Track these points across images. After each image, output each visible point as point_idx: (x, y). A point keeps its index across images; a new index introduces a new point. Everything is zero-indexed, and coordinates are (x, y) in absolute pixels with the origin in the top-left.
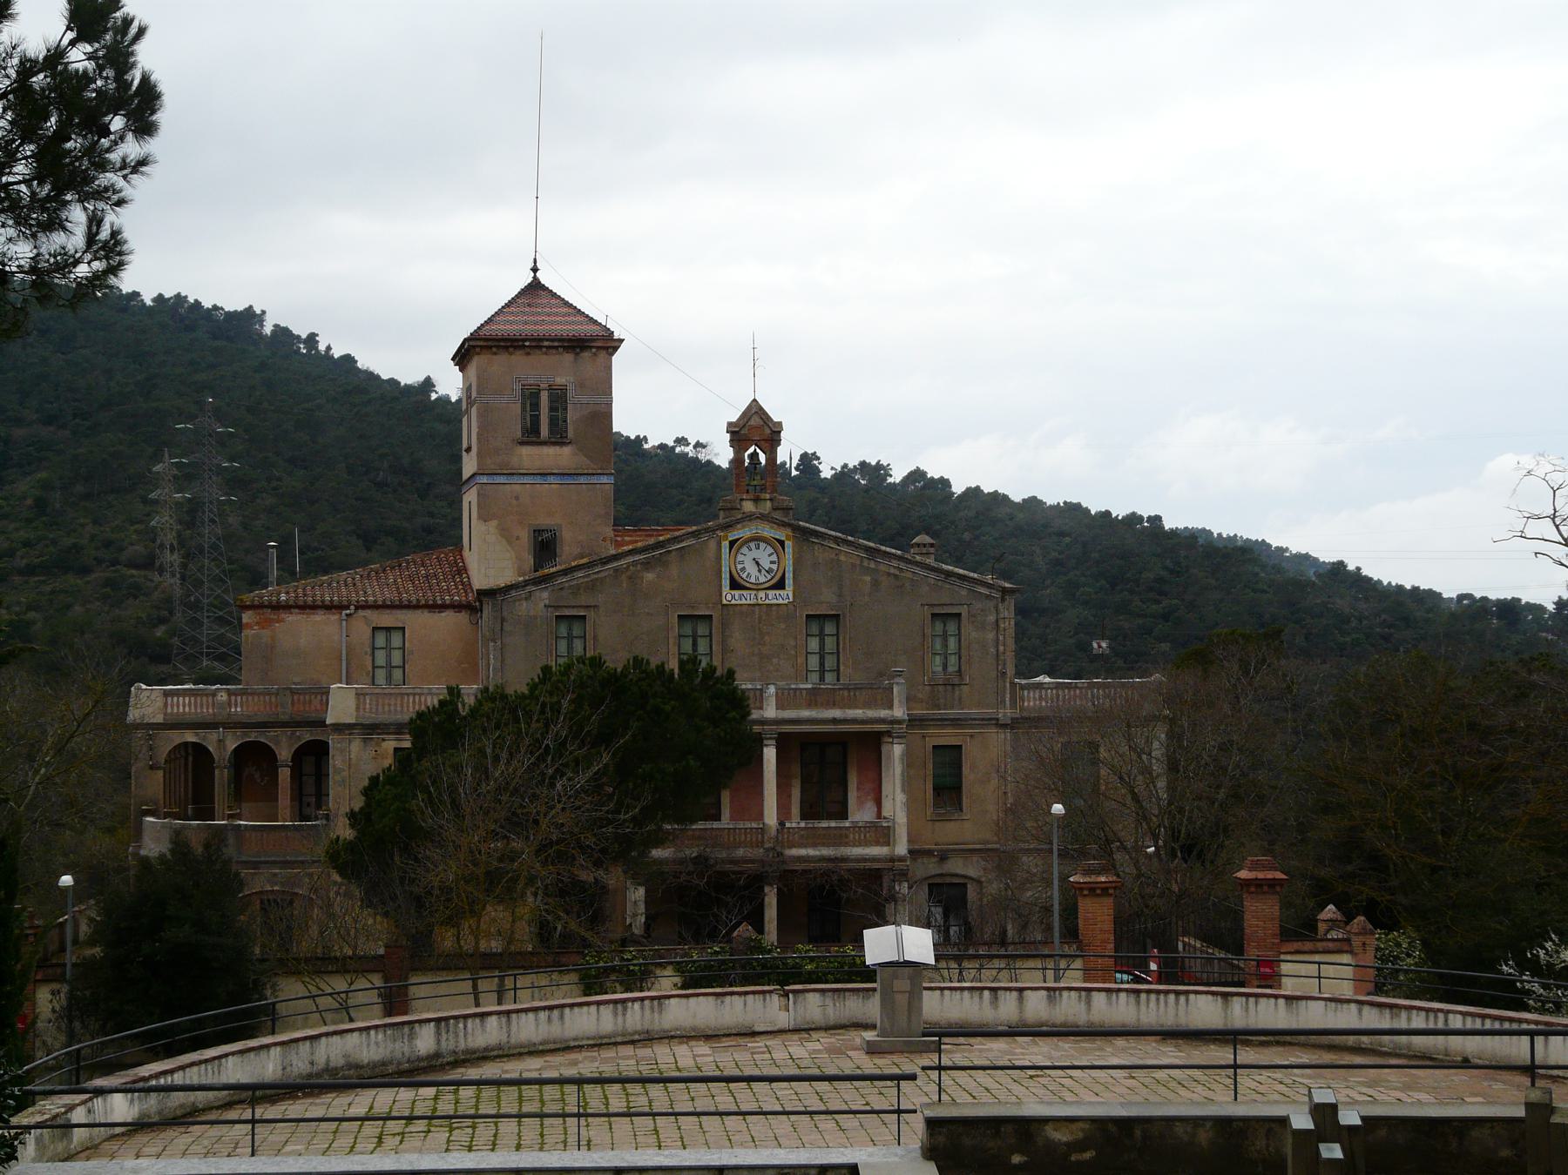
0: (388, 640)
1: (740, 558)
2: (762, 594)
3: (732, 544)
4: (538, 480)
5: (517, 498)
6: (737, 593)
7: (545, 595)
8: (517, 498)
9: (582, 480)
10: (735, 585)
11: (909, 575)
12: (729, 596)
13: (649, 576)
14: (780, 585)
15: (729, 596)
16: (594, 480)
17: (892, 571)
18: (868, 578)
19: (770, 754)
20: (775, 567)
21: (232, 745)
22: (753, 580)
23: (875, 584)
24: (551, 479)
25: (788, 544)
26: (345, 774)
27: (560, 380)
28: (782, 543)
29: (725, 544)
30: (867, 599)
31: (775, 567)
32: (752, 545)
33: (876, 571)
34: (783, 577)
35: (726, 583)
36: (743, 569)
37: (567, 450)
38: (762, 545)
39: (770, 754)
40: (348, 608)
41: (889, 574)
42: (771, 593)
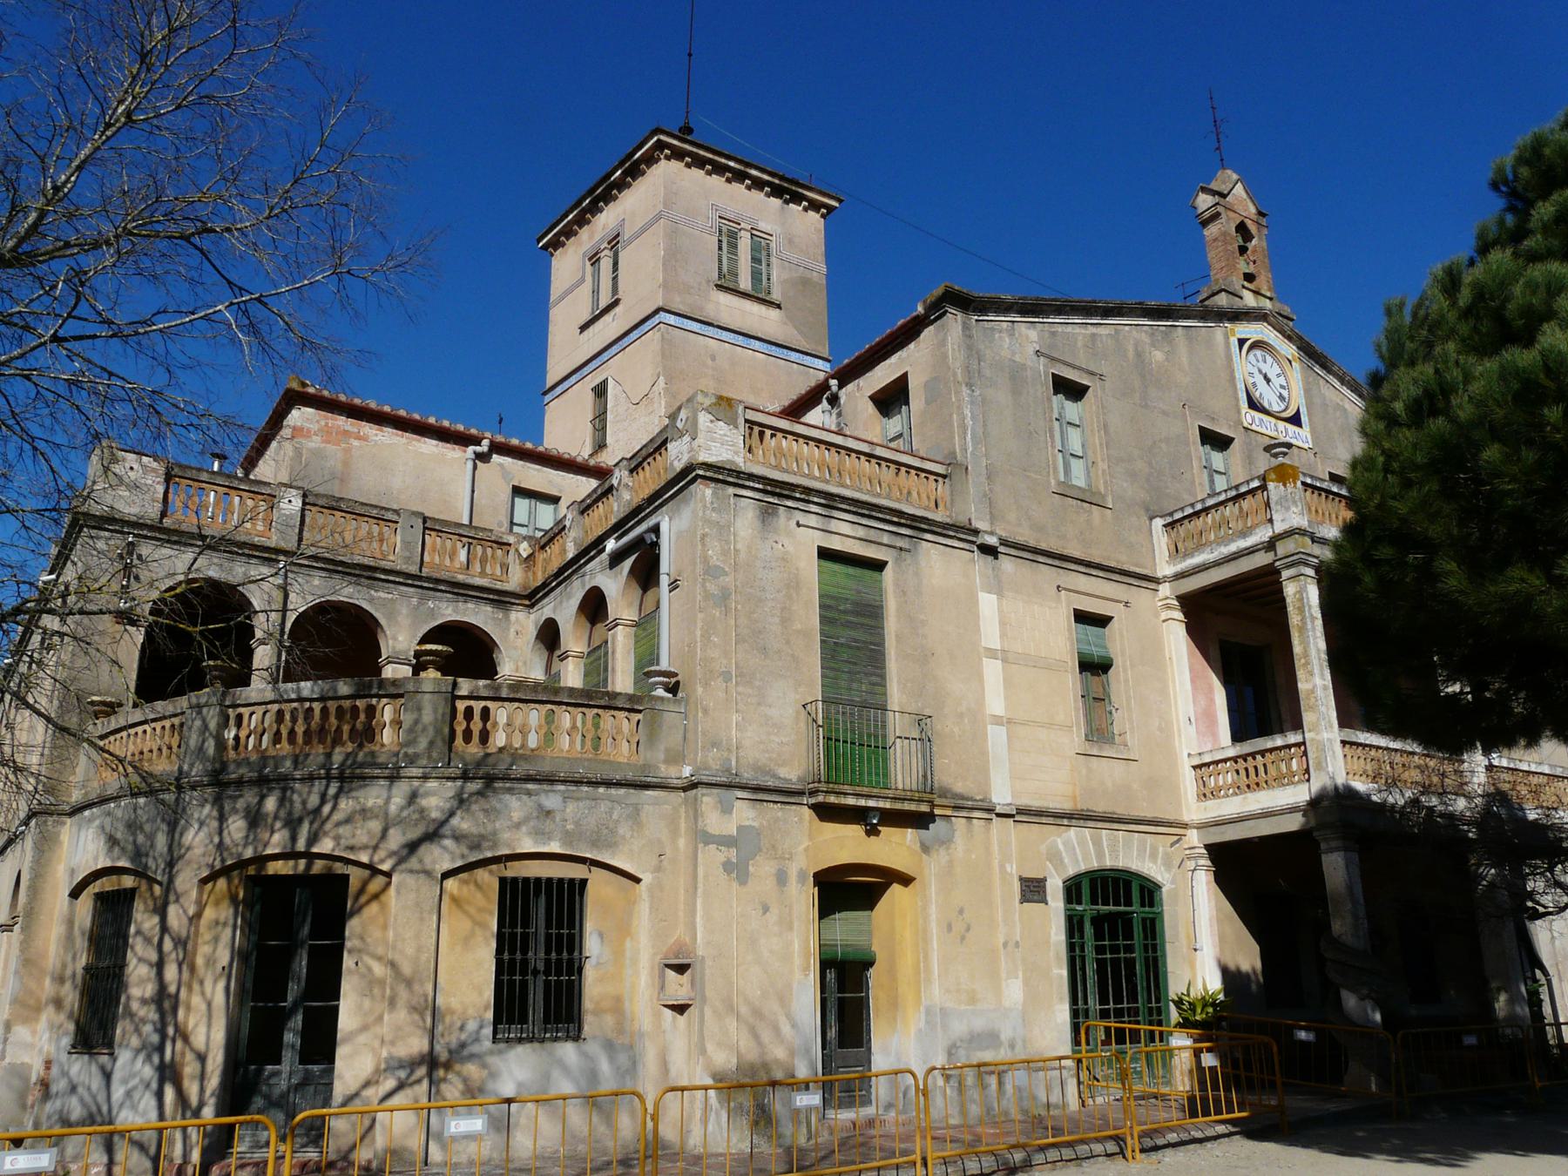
0: (532, 514)
4: (740, 340)
5: (713, 358)
7: (1033, 334)
8: (713, 358)
9: (794, 356)
13: (1158, 356)
15: (1250, 417)
16: (808, 360)
21: (299, 604)
24: (757, 345)
26: (728, 580)
27: (762, 226)
29: (1234, 341)
37: (774, 314)
40: (477, 442)
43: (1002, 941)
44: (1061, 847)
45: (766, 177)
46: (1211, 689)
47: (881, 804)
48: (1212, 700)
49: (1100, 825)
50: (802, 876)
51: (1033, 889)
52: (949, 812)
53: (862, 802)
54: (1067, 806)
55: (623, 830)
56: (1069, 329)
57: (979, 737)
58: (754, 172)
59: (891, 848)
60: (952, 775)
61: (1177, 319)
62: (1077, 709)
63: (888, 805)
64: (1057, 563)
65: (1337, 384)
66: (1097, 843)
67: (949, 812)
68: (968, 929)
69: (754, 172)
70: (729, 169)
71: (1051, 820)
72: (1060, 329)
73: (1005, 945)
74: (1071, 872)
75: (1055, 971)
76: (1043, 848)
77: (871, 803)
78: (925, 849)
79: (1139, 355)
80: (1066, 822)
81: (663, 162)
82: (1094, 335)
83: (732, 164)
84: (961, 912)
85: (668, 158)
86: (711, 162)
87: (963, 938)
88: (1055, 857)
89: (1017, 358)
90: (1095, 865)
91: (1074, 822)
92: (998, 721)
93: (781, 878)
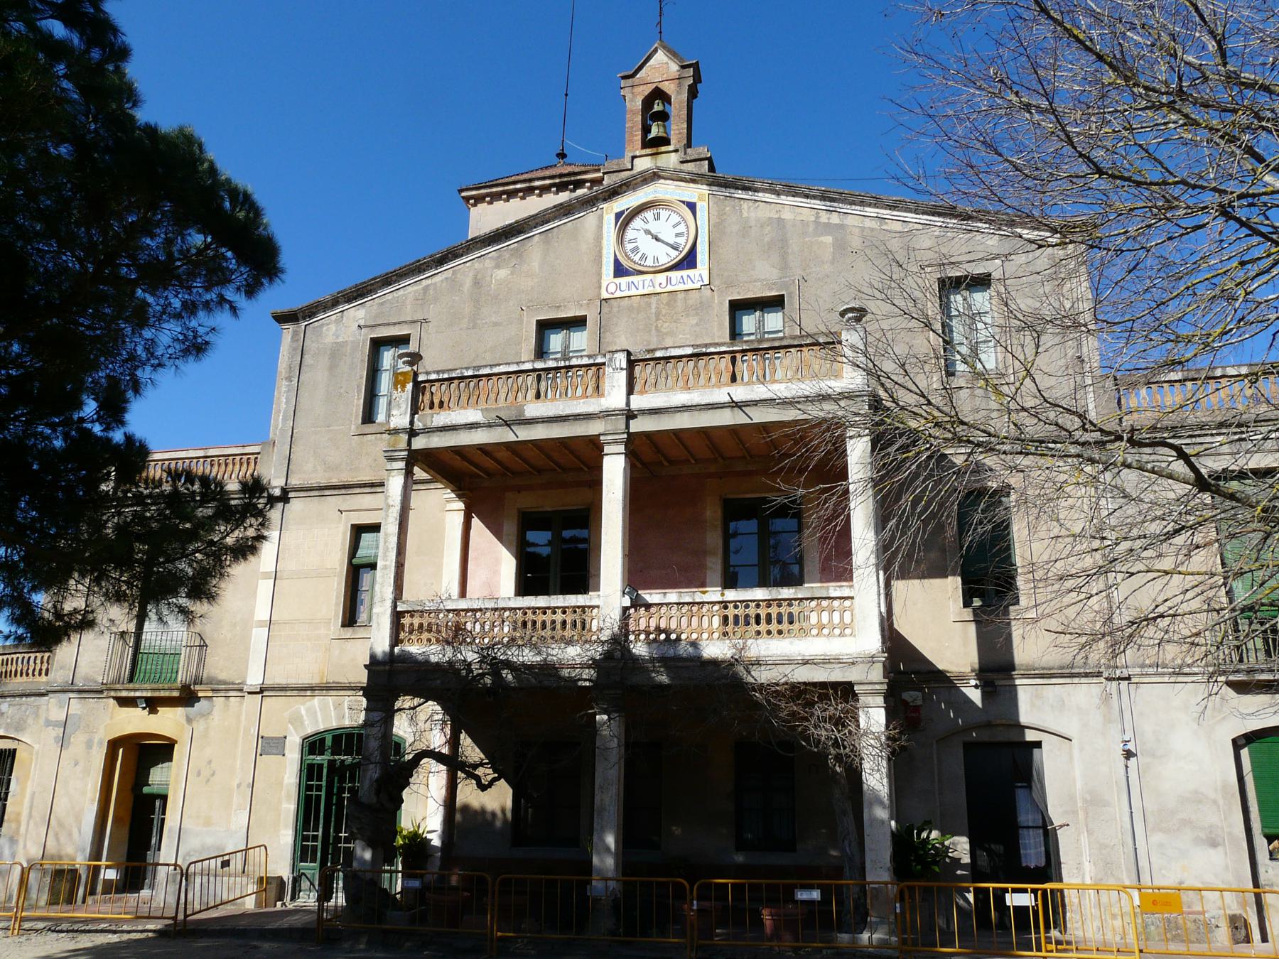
1: (630, 234)
2: (661, 278)
3: (618, 215)
6: (623, 281)
10: (620, 271)
11: (897, 226)
12: (610, 285)
13: (502, 273)
14: (689, 261)
15: (610, 285)
17: (869, 223)
18: (828, 239)
19: (614, 470)
20: (682, 240)
22: (649, 262)
23: (841, 246)
25: (702, 208)
28: (692, 207)
29: (609, 220)
30: (827, 268)
31: (682, 240)
32: (649, 215)
33: (841, 227)
34: (692, 253)
35: (608, 268)
36: (636, 250)
38: (664, 214)
39: (614, 470)
41: (863, 229)
42: (675, 275)
43: (237, 782)
44: (303, 712)
45: (548, 182)
46: (498, 561)
47: (145, 694)
48: (496, 572)
49: (342, 693)
50: (101, 743)
51: (271, 746)
52: (210, 694)
53: (132, 694)
54: (315, 681)
55: (30, 721)
56: (401, 292)
57: (245, 639)
58: (537, 183)
59: (166, 722)
60: (217, 667)
61: (531, 229)
62: (337, 604)
63: (149, 694)
64: (343, 491)
65: (770, 197)
66: (338, 706)
67: (210, 694)
68: (213, 775)
69: (537, 183)
70: (537, 188)
71: (295, 693)
72: (389, 297)
73: (239, 786)
74: (310, 730)
75: (285, 805)
76: (287, 714)
77: (138, 694)
78: (189, 720)
79: (477, 283)
80: (309, 693)
81: (472, 209)
82: (426, 288)
83: (519, 186)
84: (210, 762)
85: (475, 205)
86: (504, 192)
87: (208, 781)
88: (296, 720)
89: (340, 339)
90: (334, 725)
91: (317, 693)
92: (260, 624)
93: (89, 745)
